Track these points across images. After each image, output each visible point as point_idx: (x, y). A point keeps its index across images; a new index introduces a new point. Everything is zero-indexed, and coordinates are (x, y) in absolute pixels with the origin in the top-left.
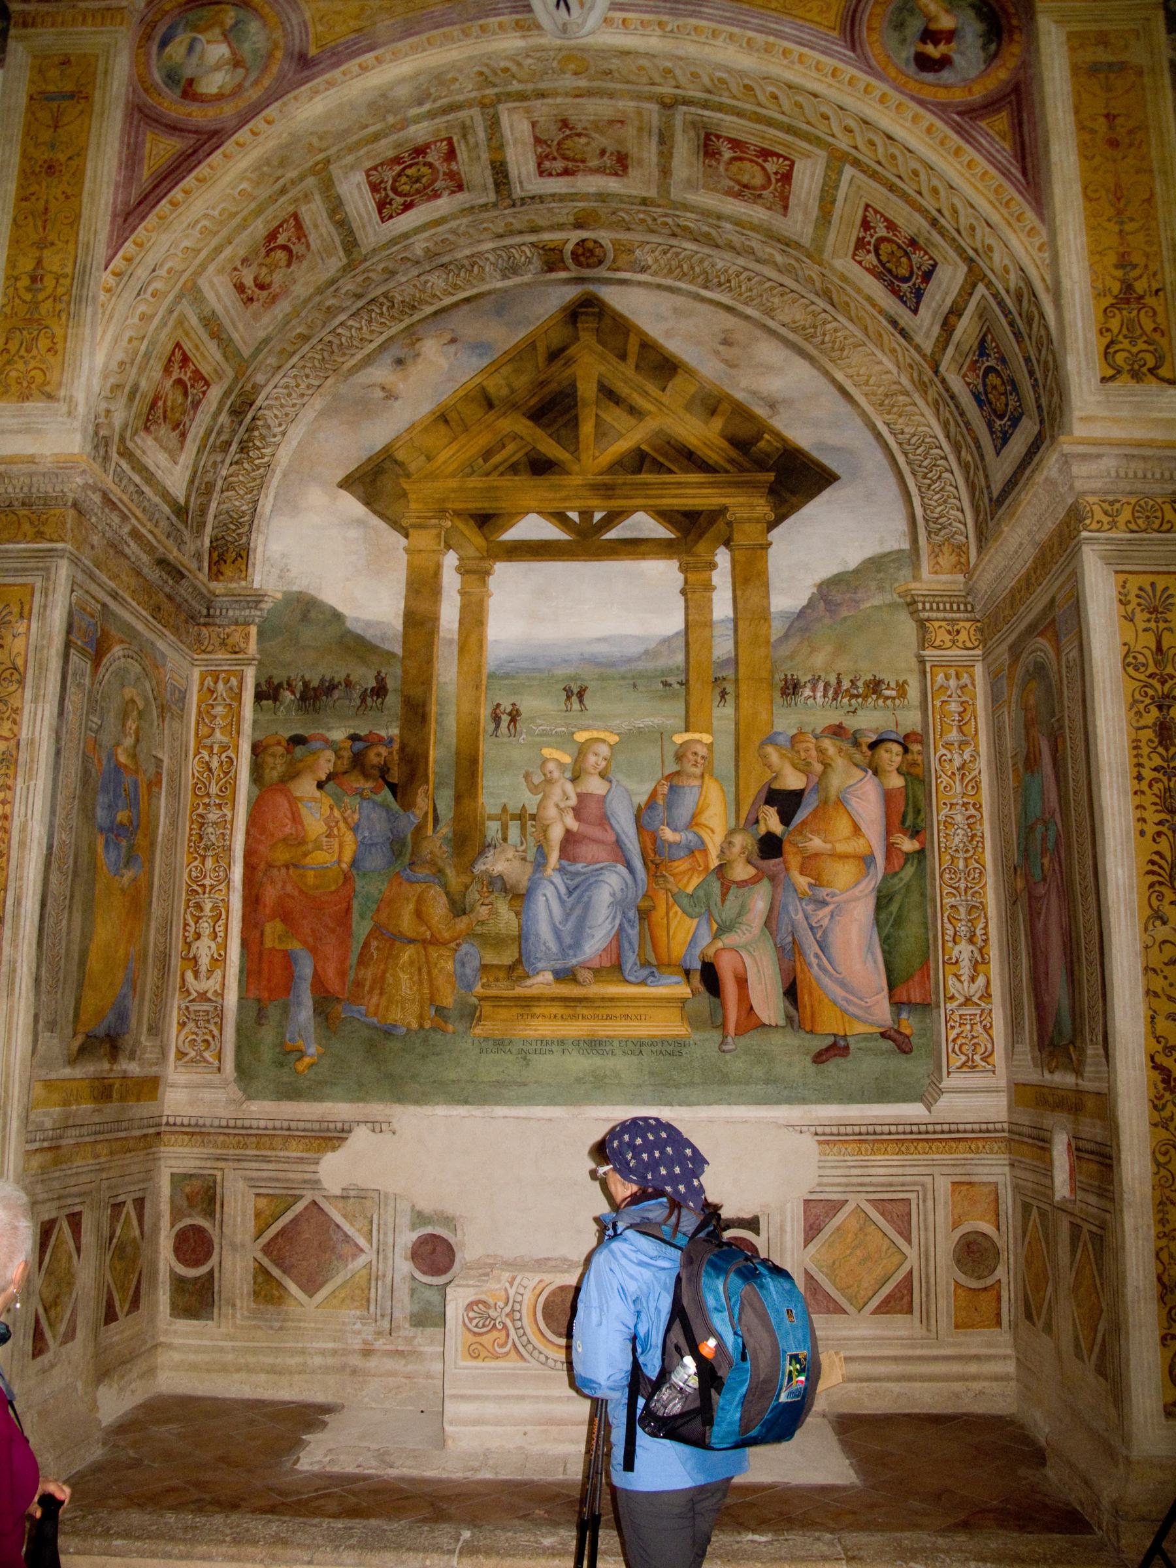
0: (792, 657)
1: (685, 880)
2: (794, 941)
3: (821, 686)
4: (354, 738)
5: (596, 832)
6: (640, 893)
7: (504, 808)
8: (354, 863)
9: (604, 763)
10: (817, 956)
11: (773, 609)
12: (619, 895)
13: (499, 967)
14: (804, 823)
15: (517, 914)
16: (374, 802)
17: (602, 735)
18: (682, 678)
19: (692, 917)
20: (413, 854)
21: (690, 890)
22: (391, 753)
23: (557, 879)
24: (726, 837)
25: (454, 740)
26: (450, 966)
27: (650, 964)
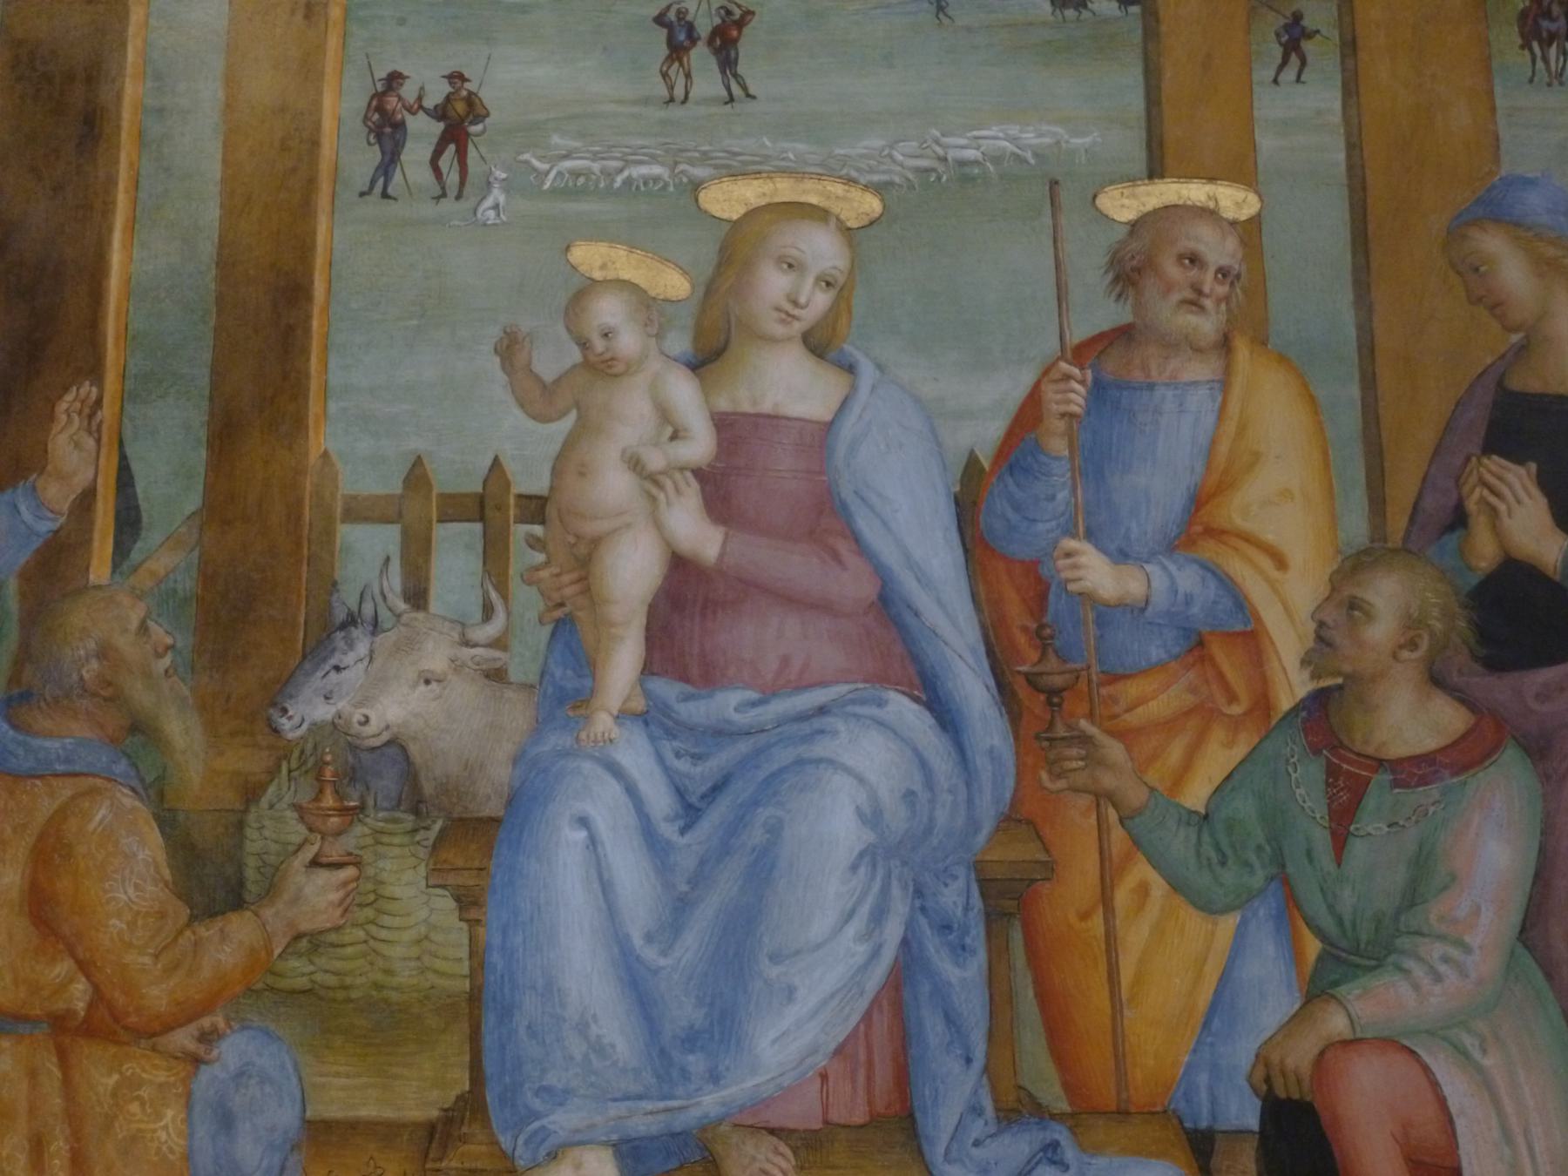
1: (1175, 752)
6: (988, 812)
7: (417, 476)
9: (821, 301)
12: (897, 819)
13: (386, 1132)
15: (468, 902)
17: (811, 194)
19: (1208, 908)
21: (1196, 795)
23: (635, 755)
25: (212, 214)
26: (167, 1128)
27: (1042, 1113)
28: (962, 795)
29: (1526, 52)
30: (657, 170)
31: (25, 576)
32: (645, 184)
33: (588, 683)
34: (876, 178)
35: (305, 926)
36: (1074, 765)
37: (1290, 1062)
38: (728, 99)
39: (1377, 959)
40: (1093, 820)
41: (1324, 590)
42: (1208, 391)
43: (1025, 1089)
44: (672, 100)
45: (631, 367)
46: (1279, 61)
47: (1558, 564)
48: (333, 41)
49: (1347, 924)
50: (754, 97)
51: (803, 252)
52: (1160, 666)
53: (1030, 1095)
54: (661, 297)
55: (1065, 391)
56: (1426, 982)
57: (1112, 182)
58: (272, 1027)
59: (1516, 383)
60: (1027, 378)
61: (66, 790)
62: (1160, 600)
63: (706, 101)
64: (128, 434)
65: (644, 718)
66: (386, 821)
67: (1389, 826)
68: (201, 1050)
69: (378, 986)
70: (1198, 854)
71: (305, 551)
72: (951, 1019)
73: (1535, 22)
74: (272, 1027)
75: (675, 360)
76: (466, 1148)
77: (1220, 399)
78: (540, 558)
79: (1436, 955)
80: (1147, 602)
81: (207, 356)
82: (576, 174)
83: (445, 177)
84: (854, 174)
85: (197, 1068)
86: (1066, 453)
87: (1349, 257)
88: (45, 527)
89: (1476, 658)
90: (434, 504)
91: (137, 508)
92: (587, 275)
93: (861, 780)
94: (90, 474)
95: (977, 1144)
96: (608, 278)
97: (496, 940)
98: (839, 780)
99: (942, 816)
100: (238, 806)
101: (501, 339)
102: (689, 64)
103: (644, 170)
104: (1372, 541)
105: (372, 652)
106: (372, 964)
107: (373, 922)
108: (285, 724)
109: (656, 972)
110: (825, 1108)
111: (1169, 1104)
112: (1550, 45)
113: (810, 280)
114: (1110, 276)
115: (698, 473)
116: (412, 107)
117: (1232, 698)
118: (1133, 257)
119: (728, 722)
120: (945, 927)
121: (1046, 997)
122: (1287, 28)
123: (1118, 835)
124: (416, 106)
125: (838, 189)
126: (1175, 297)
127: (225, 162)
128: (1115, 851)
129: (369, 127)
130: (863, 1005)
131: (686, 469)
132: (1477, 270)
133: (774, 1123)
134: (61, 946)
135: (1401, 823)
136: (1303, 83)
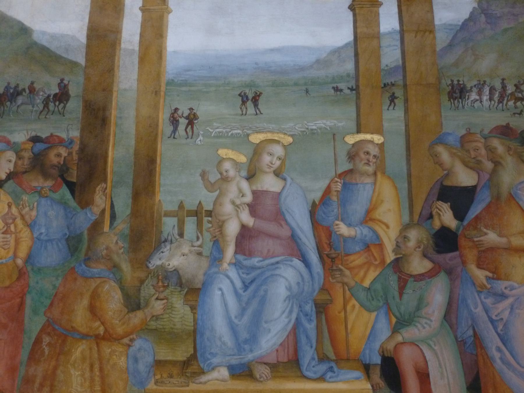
0: (456, 64)
1: (362, 273)
2: (475, 334)
3: (487, 90)
4: (35, 140)
5: (272, 228)
6: (317, 287)
7: (181, 206)
8: (29, 259)
9: (278, 163)
10: (499, 350)
11: (437, 22)
12: (295, 289)
13: (174, 363)
14: (477, 218)
15: (193, 308)
16: (52, 200)
17: (276, 137)
18: (353, 83)
19: (369, 310)
20: (89, 248)
21: (367, 283)
22: (70, 154)
23: (233, 273)
24: (401, 232)
25: (133, 142)
26: (122, 362)
27: (328, 359)
28: (311, 282)
29: (450, 101)
30: (239, 131)
31: (89, 230)
32: (236, 135)
33: (221, 256)
34: (291, 133)
35: (155, 314)
36: (338, 276)
37: (388, 348)
38: (256, 114)
39: (410, 323)
40: (342, 289)
41: (398, 234)
42: (371, 185)
43: (325, 354)
44: (242, 114)
45: (233, 179)
46: (389, 104)
47: (455, 227)
48: (162, 101)
49: (403, 315)
50: (262, 114)
51: (274, 151)
52: (359, 252)
53: (326, 355)
54: (240, 162)
55: (336, 185)
56: (421, 328)
57: (348, 134)
58: (147, 338)
59: (445, 183)
60: (327, 182)
61: (98, 281)
62: (359, 236)
63: (251, 115)
64: (113, 195)
65: (235, 264)
66: (173, 289)
67: (413, 291)
68: (130, 343)
69: (172, 328)
70: (367, 298)
71: (155, 223)
72: (307, 337)
73: (452, 95)
74: (147, 338)
75: (243, 178)
76: (192, 367)
77: (373, 187)
78: (210, 225)
79: (424, 322)
80: (356, 236)
81: (132, 177)
82: (219, 132)
83: (188, 133)
84: (286, 132)
85: (129, 349)
86: (337, 200)
87: (405, 152)
88: (94, 218)
89: (434, 250)
90: (185, 212)
91: (115, 213)
92: (222, 157)
93: (287, 280)
94: (104, 205)
95: (313, 367)
96: (227, 157)
97: (200, 317)
98: (282, 280)
99: (306, 288)
100: (139, 285)
101: (202, 172)
102: (247, 106)
103: (236, 131)
104: (410, 222)
105: (170, 248)
106: (170, 323)
107: (171, 313)
108: (150, 265)
109: (237, 325)
110: (278, 359)
111: (359, 357)
112: (455, 100)
113: (275, 158)
114: (347, 157)
115: (248, 205)
116: (180, 116)
117: (376, 260)
118: (353, 153)
119: (255, 265)
120: (306, 315)
121: (330, 332)
122: (391, 96)
123: (348, 293)
124: (181, 116)
125: (282, 136)
126: (363, 162)
127: (136, 130)
128: (347, 297)
129: (170, 121)
130: (286, 333)
131: (245, 204)
132: (436, 156)
133: (265, 362)
134: (97, 319)
135: (416, 290)
136: (395, 110)
